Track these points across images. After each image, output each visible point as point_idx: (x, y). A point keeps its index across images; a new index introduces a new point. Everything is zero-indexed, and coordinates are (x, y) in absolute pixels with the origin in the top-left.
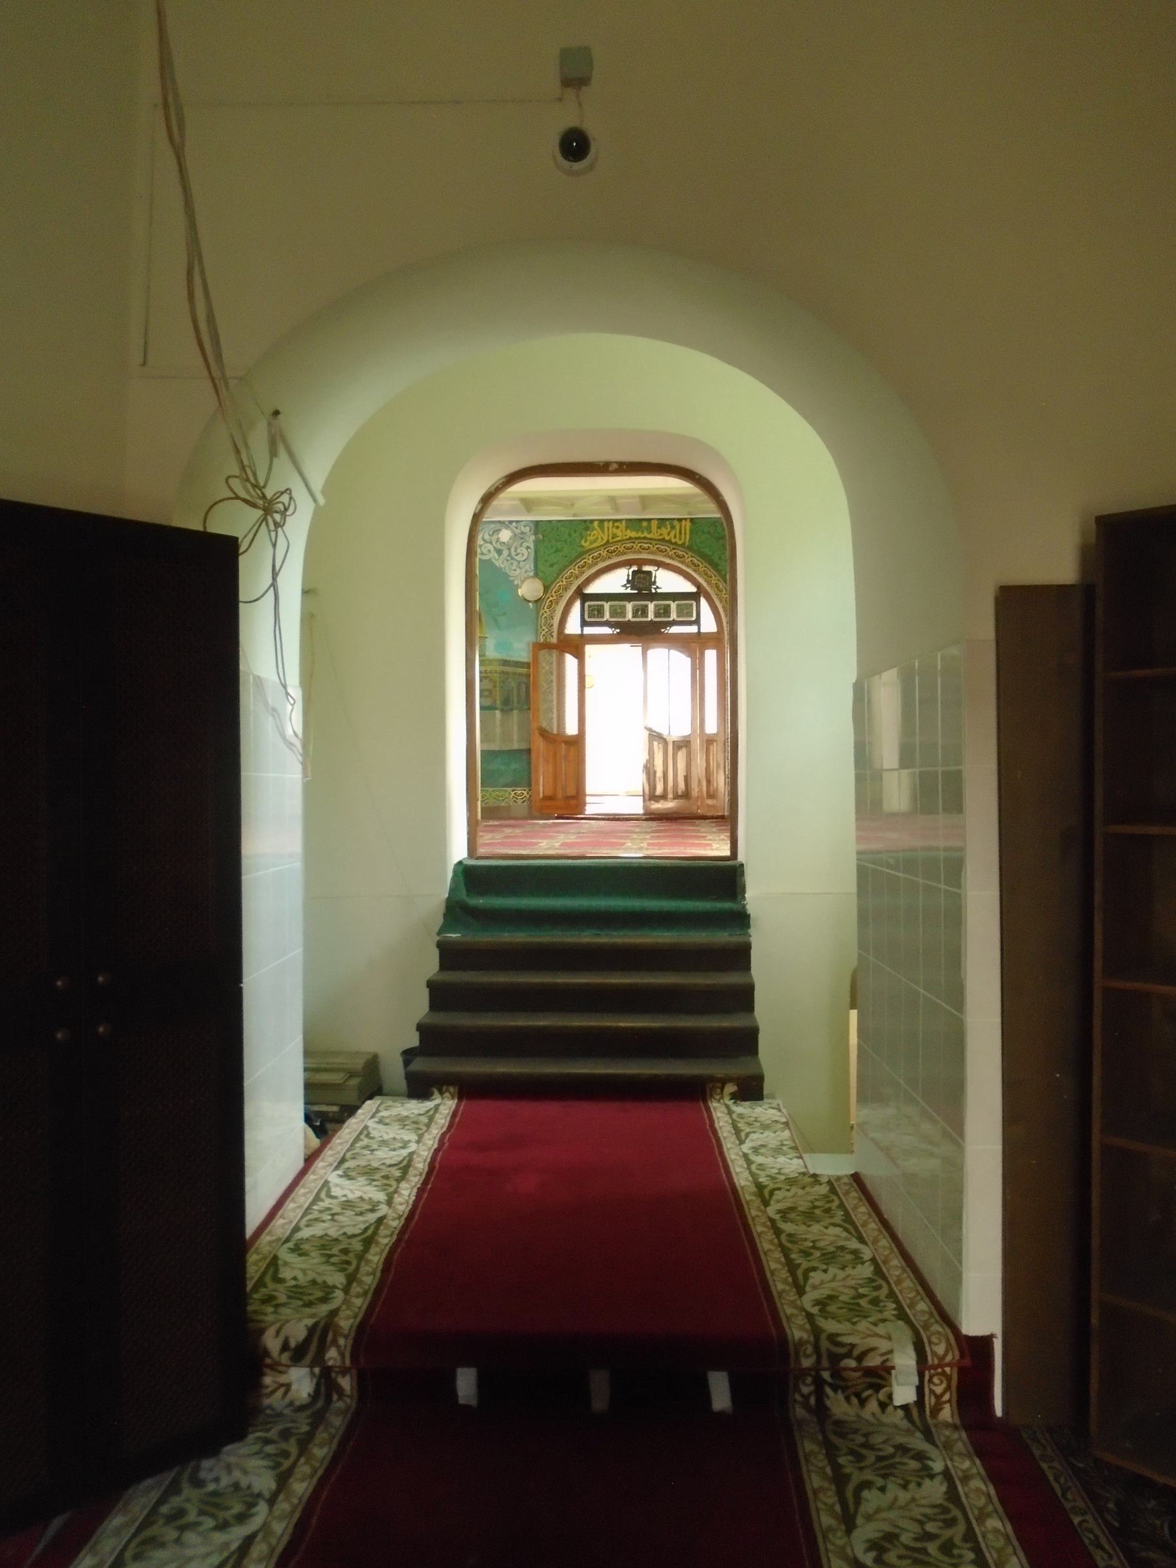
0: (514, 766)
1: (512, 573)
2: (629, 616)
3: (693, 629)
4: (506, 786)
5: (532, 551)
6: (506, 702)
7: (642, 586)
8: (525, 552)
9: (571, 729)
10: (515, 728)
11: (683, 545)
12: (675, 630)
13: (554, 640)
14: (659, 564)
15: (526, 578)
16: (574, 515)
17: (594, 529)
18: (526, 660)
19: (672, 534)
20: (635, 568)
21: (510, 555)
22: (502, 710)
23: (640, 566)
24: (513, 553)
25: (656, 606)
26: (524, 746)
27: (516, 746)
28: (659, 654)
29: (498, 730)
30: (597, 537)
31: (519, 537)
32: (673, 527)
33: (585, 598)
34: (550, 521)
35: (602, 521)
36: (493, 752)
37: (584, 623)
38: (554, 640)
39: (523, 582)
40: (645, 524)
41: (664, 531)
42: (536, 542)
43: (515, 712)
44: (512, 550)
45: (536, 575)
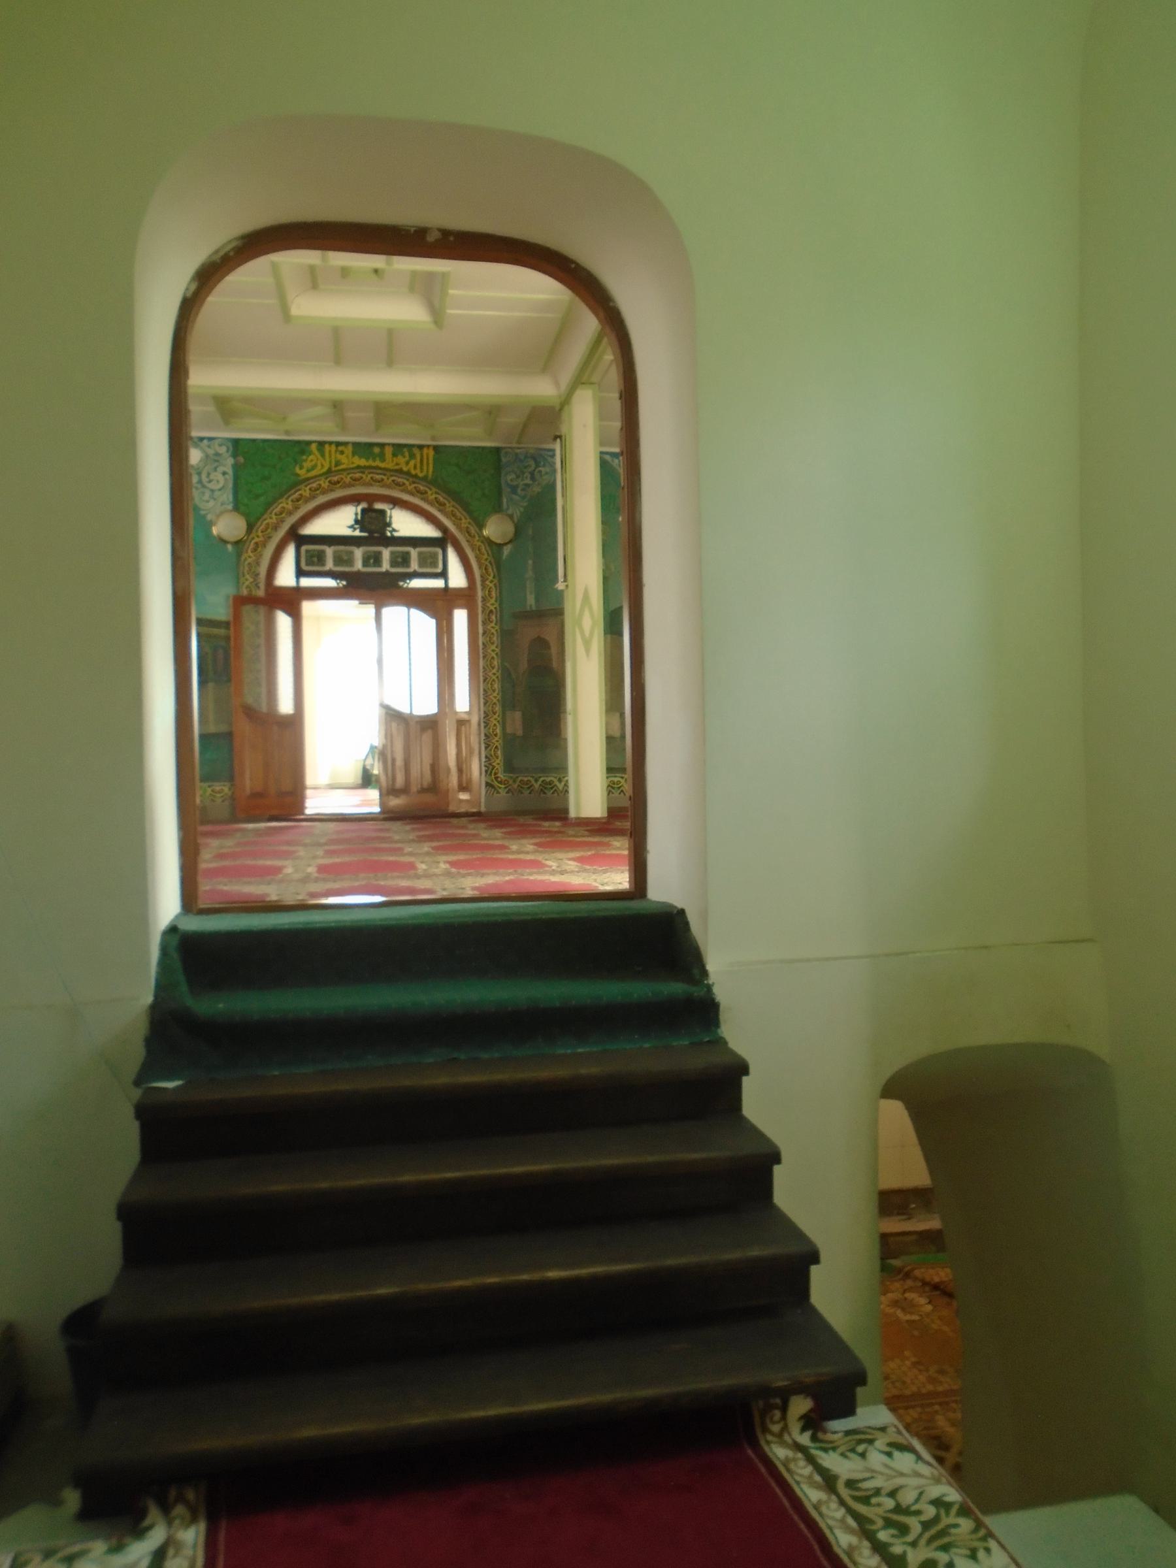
2: (358, 565)
3: (439, 583)
7: (374, 527)
9: (285, 706)
11: (425, 479)
12: (417, 583)
13: (261, 593)
14: (396, 503)
15: (222, 513)
16: (287, 432)
17: (311, 453)
19: (412, 463)
20: (364, 505)
21: (200, 482)
23: (370, 503)
25: (392, 553)
26: (223, 728)
28: (395, 614)
30: (315, 464)
32: (412, 456)
33: (301, 541)
34: (254, 441)
35: (321, 444)
37: (300, 573)
38: (261, 593)
39: (218, 516)
40: (377, 450)
41: (401, 460)
42: (236, 467)
44: (204, 476)
45: (236, 508)
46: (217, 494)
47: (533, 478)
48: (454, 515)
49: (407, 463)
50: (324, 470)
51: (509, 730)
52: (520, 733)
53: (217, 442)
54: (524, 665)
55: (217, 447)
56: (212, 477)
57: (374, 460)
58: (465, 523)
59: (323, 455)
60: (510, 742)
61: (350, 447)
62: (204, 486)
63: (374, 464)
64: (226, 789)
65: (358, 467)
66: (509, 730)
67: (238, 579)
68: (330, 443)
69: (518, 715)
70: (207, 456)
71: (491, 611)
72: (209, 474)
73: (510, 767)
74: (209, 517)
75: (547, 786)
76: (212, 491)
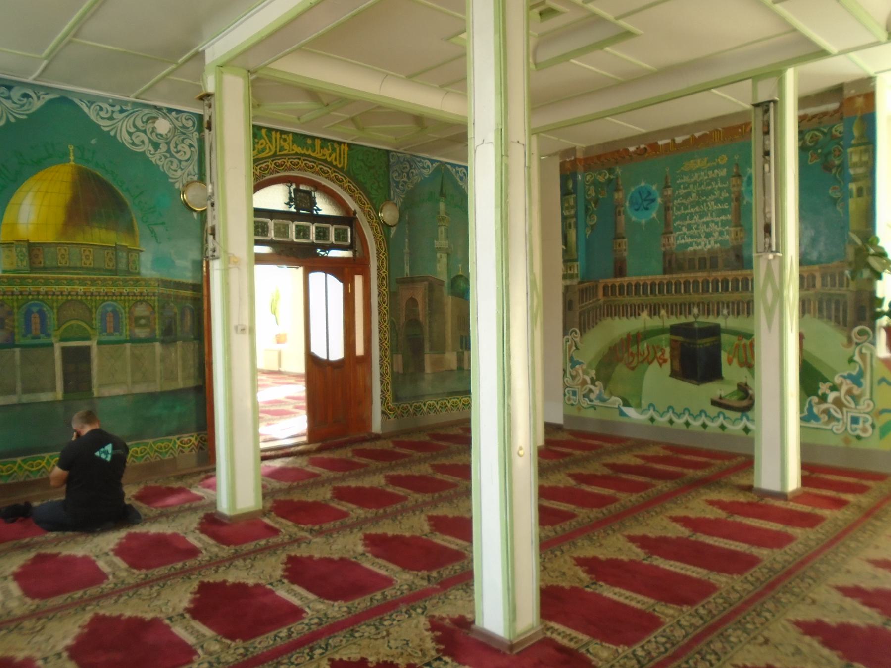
1: (170, 174)
2: (292, 236)
4: (170, 434)
11: (341, 169)
12: (334, 254)
17: (262, 137)
18: (190, 281)
19: (333, 156)
21: (169, 151)
22: (163, 342)
23: (298, 185)
27: (180, 384)
28: (317, 278)
29: (159, 367)
31: (179, 131)
32: (334, 150)
35: (270, 130)
40: (309, 141)
43: (179, 343)
44: (172, 146)
46: (184, 163)
47: (408, 178)
48: (360, 201)
49: (330, 156)
50: (272, 153)
51: (395, 370)
52: (401, 371)
53: (185, 115)
54: (403, 319)
55: (184, 120)
56: (179, 148)
57: (307, 150)
58: (367, 207)
59: (271, 141)
60: (395, 377)
61: (290, 135)
62: (172, 156)
63: (307, 153)
64: (193, 439)
65: (296, 154)
66: (395, 370)
68: (277, 130)
69: (400, 357)
70: (175, 128)
71: (383, 278)
72: (177, 145)
73: (396, 398)
74: (177, 186)
75: (418, 409)
76: (180, 161)
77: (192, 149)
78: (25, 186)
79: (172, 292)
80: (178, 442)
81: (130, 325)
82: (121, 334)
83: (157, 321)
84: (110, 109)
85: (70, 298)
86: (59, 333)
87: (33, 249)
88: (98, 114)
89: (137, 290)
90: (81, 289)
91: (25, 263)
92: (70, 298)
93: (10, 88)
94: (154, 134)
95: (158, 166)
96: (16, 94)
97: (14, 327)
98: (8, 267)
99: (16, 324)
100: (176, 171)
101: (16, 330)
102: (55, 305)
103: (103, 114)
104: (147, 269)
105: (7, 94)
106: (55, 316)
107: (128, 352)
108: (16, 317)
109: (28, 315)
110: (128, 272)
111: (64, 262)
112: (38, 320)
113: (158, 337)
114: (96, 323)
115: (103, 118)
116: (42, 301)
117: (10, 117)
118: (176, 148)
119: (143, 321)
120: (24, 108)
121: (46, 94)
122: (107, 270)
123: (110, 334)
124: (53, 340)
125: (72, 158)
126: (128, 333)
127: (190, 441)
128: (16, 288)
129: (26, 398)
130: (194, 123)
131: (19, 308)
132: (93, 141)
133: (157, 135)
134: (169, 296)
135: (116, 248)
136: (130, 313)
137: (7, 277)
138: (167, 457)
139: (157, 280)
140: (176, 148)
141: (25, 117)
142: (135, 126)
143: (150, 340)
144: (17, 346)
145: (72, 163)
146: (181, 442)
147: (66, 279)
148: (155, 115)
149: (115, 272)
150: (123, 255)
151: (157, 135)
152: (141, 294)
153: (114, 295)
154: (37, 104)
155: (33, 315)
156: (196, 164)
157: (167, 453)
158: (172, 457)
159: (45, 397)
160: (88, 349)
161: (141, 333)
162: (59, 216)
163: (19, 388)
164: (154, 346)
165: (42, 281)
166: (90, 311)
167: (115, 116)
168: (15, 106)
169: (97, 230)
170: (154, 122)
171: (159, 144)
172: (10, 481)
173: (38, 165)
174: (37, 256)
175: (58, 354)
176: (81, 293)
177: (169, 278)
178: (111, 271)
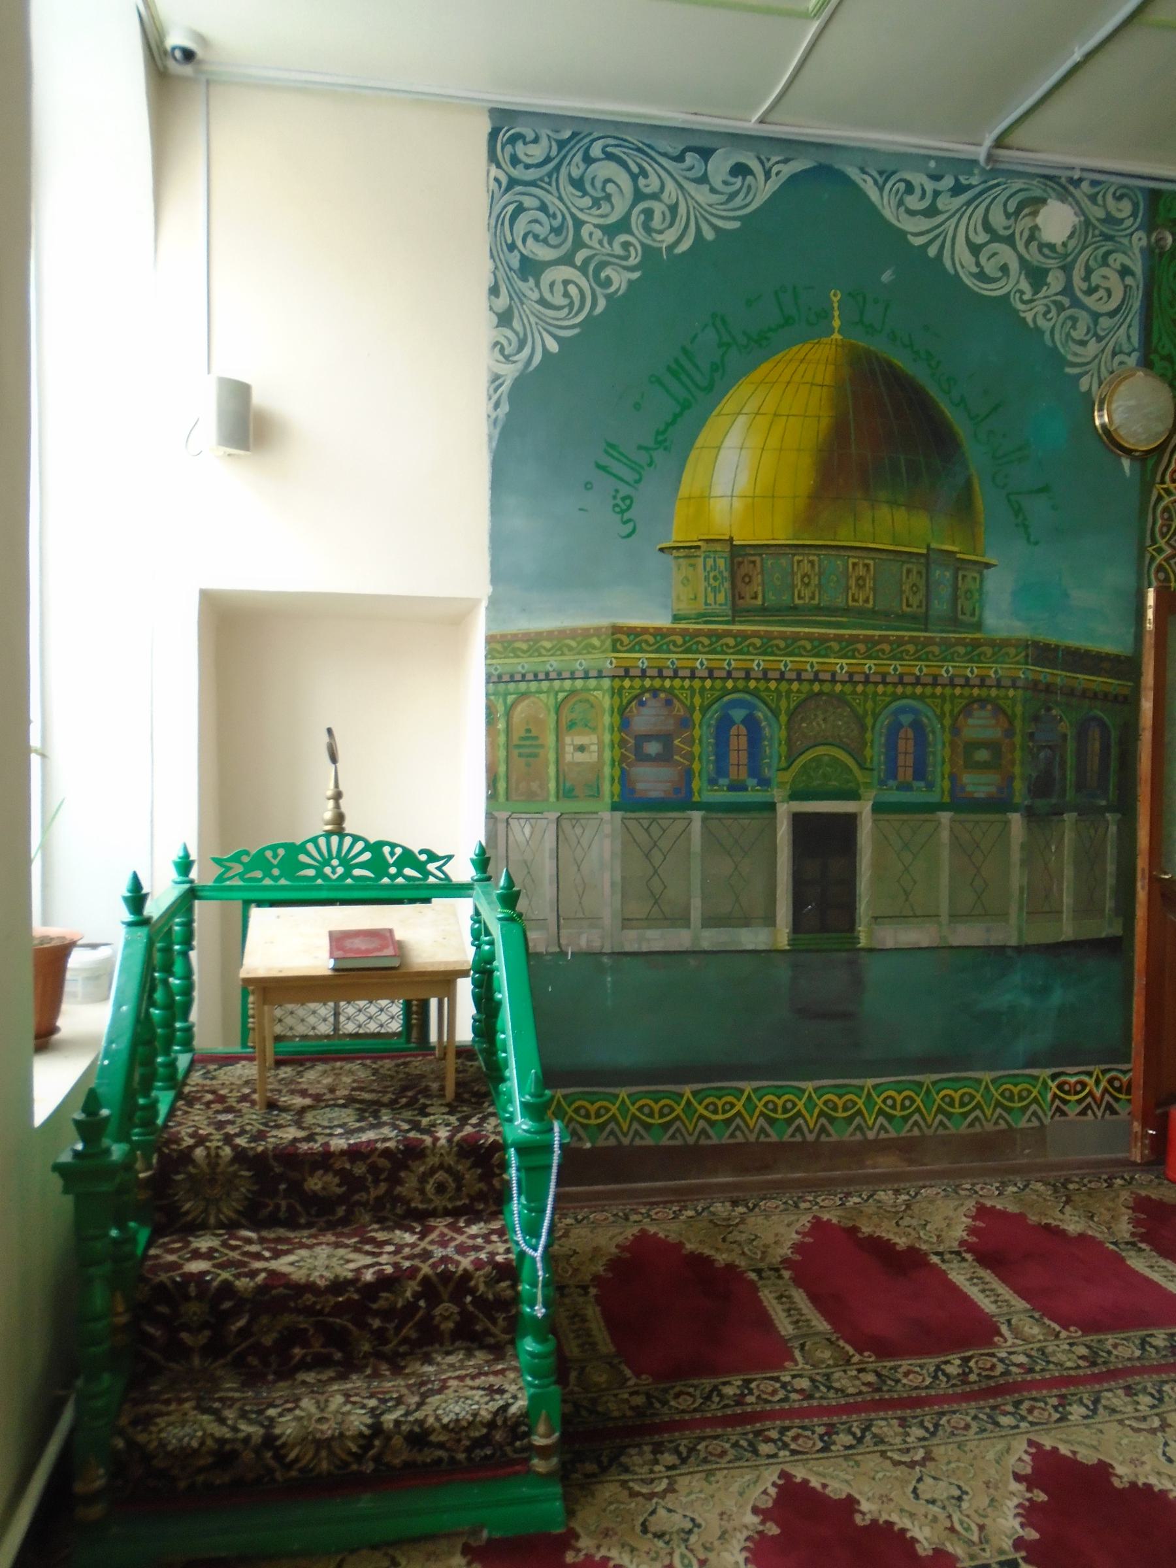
0: (1057, 997)
1: (1071, 352)
4: (1033, 1062)
5: (1137, 282)
6: (1042, 786)
8: (1115, 286)
10: (1068, 872)
21: (1068, 290)
22: (1030, 814)
24: (1078, 284)
27: (1067, 931)
29: (1017, 878)
31: (1096, 233)
36: (1001, 949)
42: (1153, 254)
43: (1069, 817)
44: (1078, 273)
46: (1105, 322)
56: (1095, 279)
62: (1076, 303)
64: (1091, 1082)
67: (1142, 549)
70: (1087, 223)
72: (1089, 271)
76: (1096, 316)
77: (1129, 280)
78: (728, 405)
79: (1060, 677)
80: (1053, 1085)
81: (953, 763)
82: (930, 786)
83: (1018, 754)
84: (930, 186)
85: (816, 687)
86: (787, 776)
87: (739, 557)
88: (901, 203)
89: (972, 671)
90: (841, 665)
91: (721, 598)
92: (816, 687)
93: (706, 153)
94: (1034, 246)
95: (1039, 331)
96: (719, 167)
97: (690, 757)
98: (684, 607)
99: (697, 749)
100: (1083, 343)
101: (696, 766)
102: (783, 704)
103: (913, 202)
104: (1002, 615)
105: (697, 173)
106: (783, 734)
107: (945, 835)
108: (697, 732)
109: (724, 725)
110: (954, 622)
111: (806, 593)
112: (744, 741)
113: (1017, 799)
114: (875, 753)
115: (911, 213)
116: (755, 693)
117: (705, 227)
118: (1087, 278)
119: (982, 755)
120: (731, 205)
121: (786, 161)
122: (902, 616)
123: (905, 787)
124: (777, 794)
125: (836, 323)
126: (947, 784)
127: (1084, 1085)
128: (700, 661)
129: (710, 939)
130: (1136, 206)
131: (704, 710)
132: (886, 277)
133: (1041, 246)
134: (1049, 689)
135: (927, 559)
136: (956, 730)
137: (684, 633)
138: (1023, 1124)
139: (1025, 645)
140: (1087, 278)
141: (736, 225)
142: (987, 226)
143: (999, 804)
144: (697, 806)
145: (836, 336)
146: (1060, 1087)
147: (809, 637)
148: (1038, 193)
149: (922, 620)
150: (942, 575)
151: (1041, 246)
152: (983, 682)
153: (918, 682)
154: (764, 190)
155: (734, 731)
156: (1136, 323)
157: (1024, 1109)
158: (1035, 1123)
159: (752, 938)
160: (849, 822)
161: (979, 785)
162: (800, 477)
163: (696, 915)
164: (1007, 823)
165: (758, 642)
166: (863, 728)
167: (940, 204)
168: (715, 198)
169: (884, 511)
170: (1035, 214)
171: (1046, 272)
172: (665, 1141)
173: (760, 345)
174: (748, 579)
175: (784, 830)
176: (842, 675)
177: (1053, 640)
178: (914, 618)
